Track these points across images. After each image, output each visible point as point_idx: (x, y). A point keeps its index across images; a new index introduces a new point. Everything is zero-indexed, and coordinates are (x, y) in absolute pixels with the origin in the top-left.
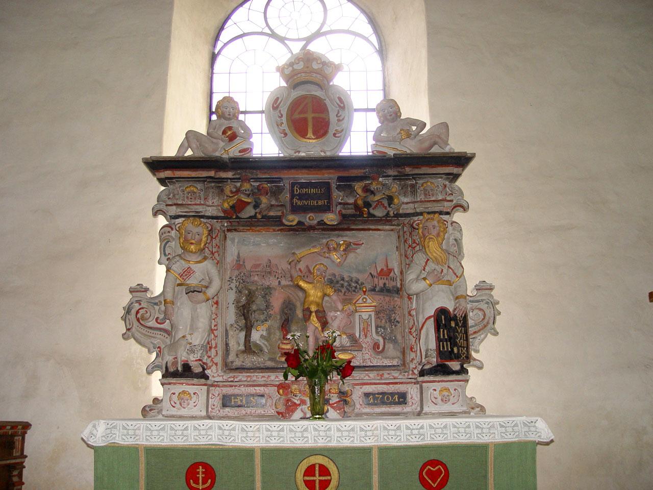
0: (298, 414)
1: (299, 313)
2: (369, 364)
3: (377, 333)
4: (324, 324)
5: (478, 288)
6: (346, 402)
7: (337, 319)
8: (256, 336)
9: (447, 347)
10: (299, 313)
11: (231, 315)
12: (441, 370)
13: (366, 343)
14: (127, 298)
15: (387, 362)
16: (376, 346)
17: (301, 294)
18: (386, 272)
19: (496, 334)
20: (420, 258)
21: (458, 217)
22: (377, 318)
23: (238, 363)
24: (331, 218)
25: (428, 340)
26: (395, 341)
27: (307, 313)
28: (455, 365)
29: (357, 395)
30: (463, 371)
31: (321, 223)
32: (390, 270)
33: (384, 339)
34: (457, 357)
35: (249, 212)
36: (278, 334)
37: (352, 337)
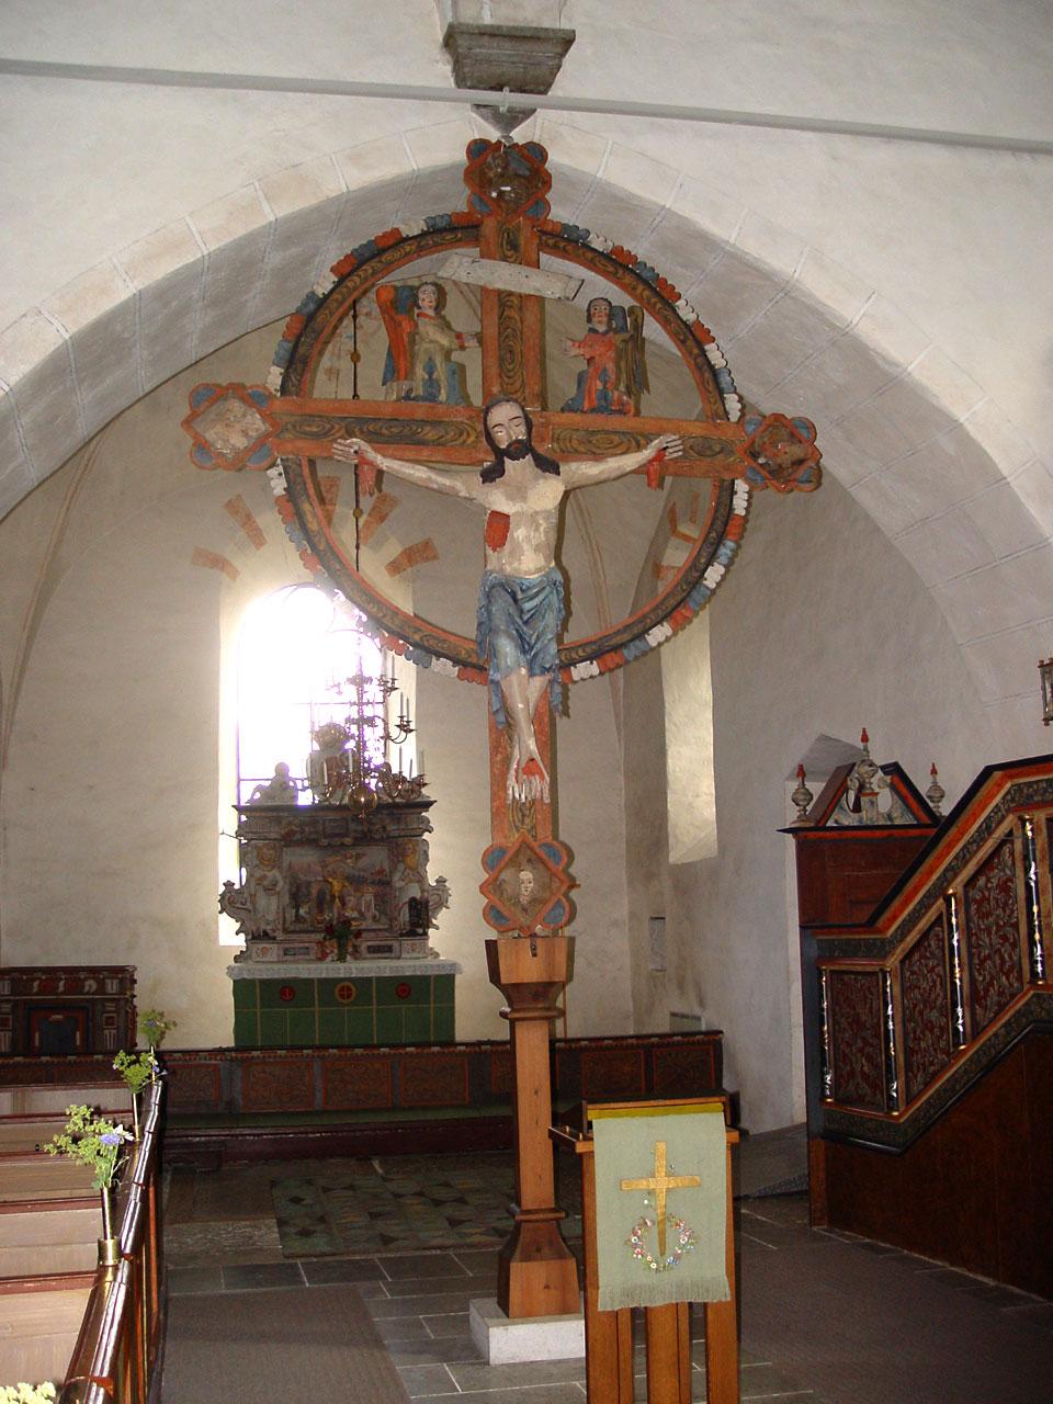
0: (330, 958)
1: (328, 898)
2: (370, 928)
3: (376, 909)
4: (344, 904)
5: (437, 881)
6: (357, 951)
7: (351, 900)
8: (302, 911)
9: (416, 920)
10: (328, 898)
11: (286, 899)
12: (412, 933)
13: (368, 915)
14: (222, 889)
15: (381, 927)
16: (375, 917)
17: (329, 886)
18: (381, 871)
19: (448, 908)
20: (401, 867)
21: (426, 836)
22: (376, 900)
23: (292, 928)
24: (348, 841)
25: (405, 916)
26: (386, 914)
27: (333, 897)
28: (420, 931)
29: (363, 947)
30: (426, 934)
31: (343, 844)
32: (384, 870)
33: (380, 913)
34: (420, 926)
35: (298, 836)
36: (315, 911)
37: (360, 912)
